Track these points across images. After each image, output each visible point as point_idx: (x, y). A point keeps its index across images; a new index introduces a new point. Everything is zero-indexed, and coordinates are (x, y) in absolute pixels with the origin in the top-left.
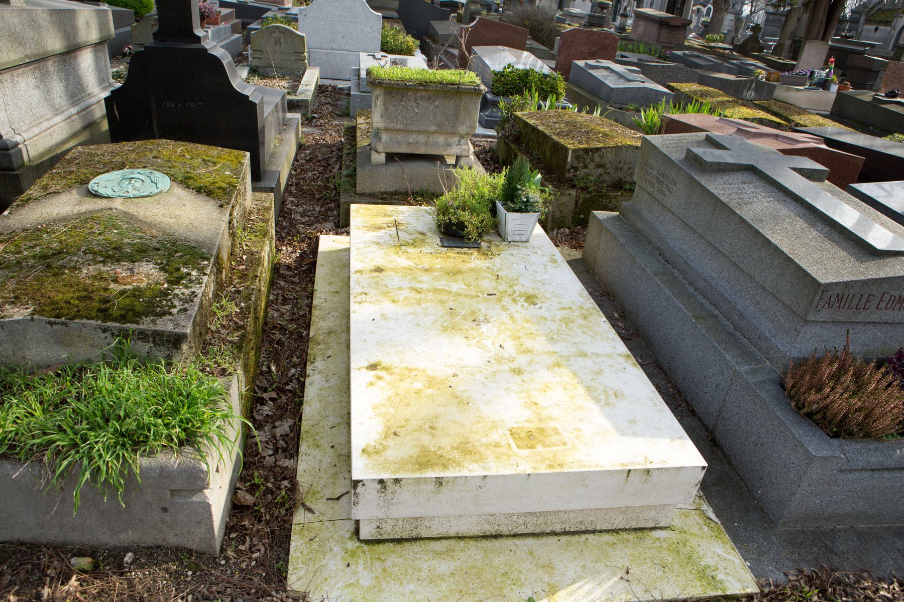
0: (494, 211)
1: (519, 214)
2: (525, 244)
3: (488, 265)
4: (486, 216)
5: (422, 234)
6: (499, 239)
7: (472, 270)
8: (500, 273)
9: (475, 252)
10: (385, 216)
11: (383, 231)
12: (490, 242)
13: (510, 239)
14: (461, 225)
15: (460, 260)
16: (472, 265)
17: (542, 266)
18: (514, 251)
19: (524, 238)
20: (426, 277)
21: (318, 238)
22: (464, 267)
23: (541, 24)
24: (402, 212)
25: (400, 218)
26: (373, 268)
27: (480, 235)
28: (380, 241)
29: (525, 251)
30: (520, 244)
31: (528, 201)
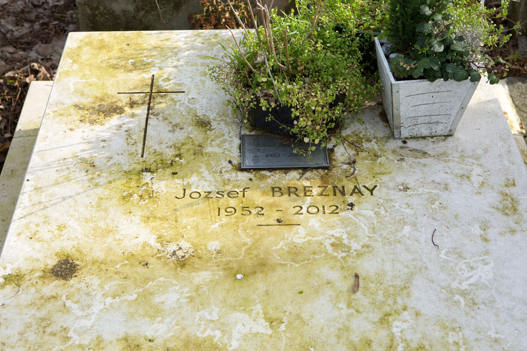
0: (370, 67)
1: (425, 83)
2: (442, 146)
3: (338, 232)
4: (349, 82)
5: (203, 124)
6: (381, 131)
7: (295, 253)
8: (367, 267)
9: (311, 181)
10: (135, 67)
11: (115, 120)
12: (356, 145)
13: (405, 133)
14: (283, 113)
15: (273, 216)
16: (298, 236)
17: (476, 230)
18: (410, 173)
19: (440, 129)
20: (172, 294)
21: (26, 86)
22: (277, 242)
23: (110, 117)
24: (175, 51)
25: (166, 73)
26: (52, 262)
27: (334, 127)
28: (100, 157)
29: (437, 171)
30: (429, 146)
31: (448, 49)
